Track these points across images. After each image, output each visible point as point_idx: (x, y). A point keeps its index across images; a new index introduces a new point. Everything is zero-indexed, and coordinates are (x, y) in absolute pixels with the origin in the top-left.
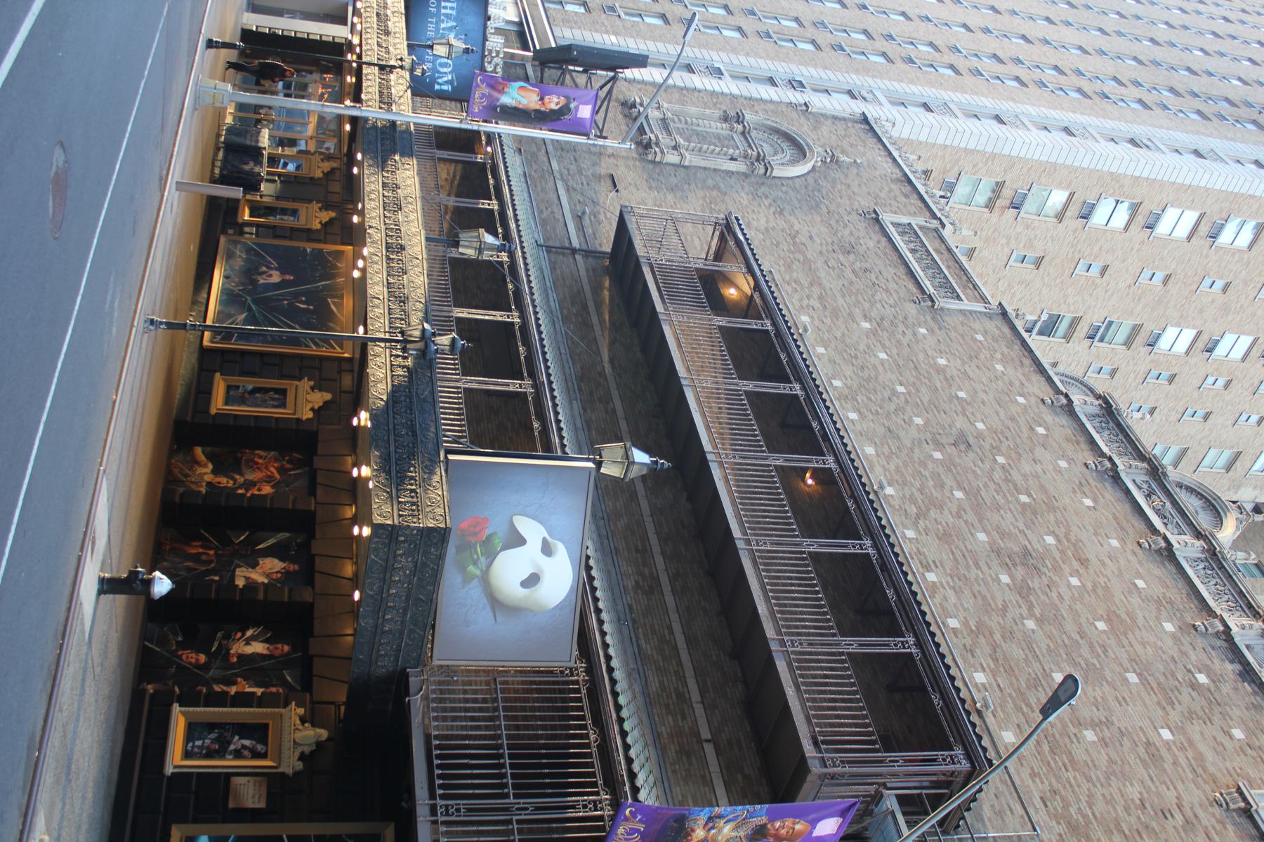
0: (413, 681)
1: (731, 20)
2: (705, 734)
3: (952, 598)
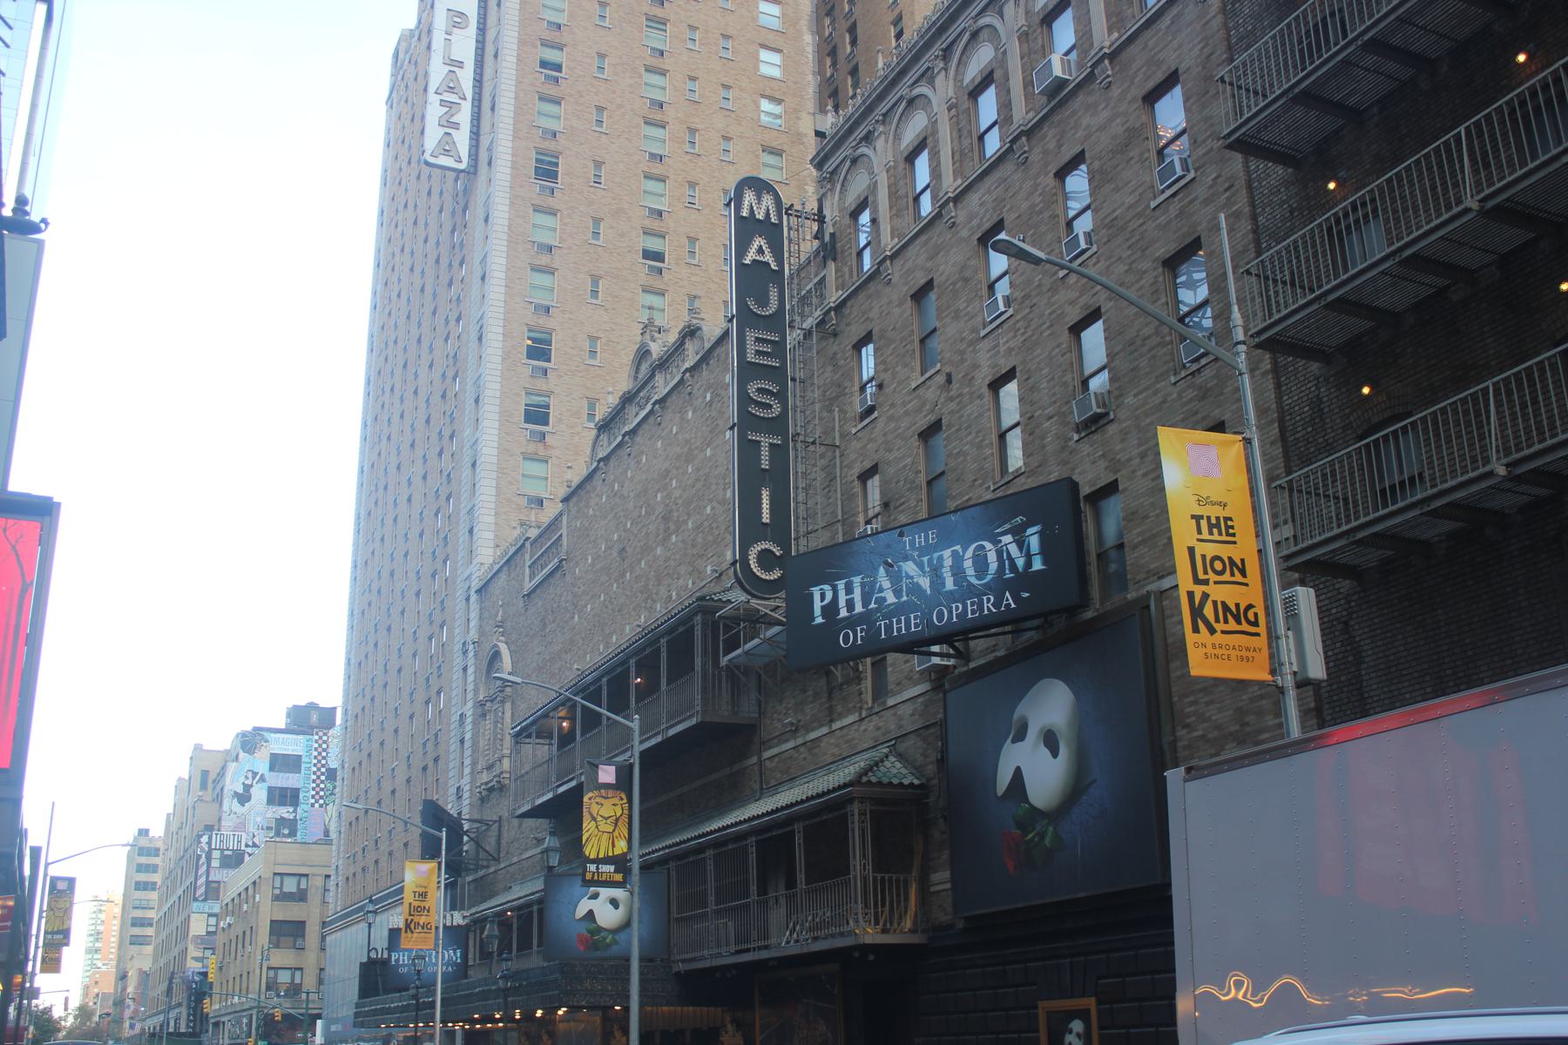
0: (681, 967)
1: (434, 699)
2: (727, 771)
3: (681, 582)
